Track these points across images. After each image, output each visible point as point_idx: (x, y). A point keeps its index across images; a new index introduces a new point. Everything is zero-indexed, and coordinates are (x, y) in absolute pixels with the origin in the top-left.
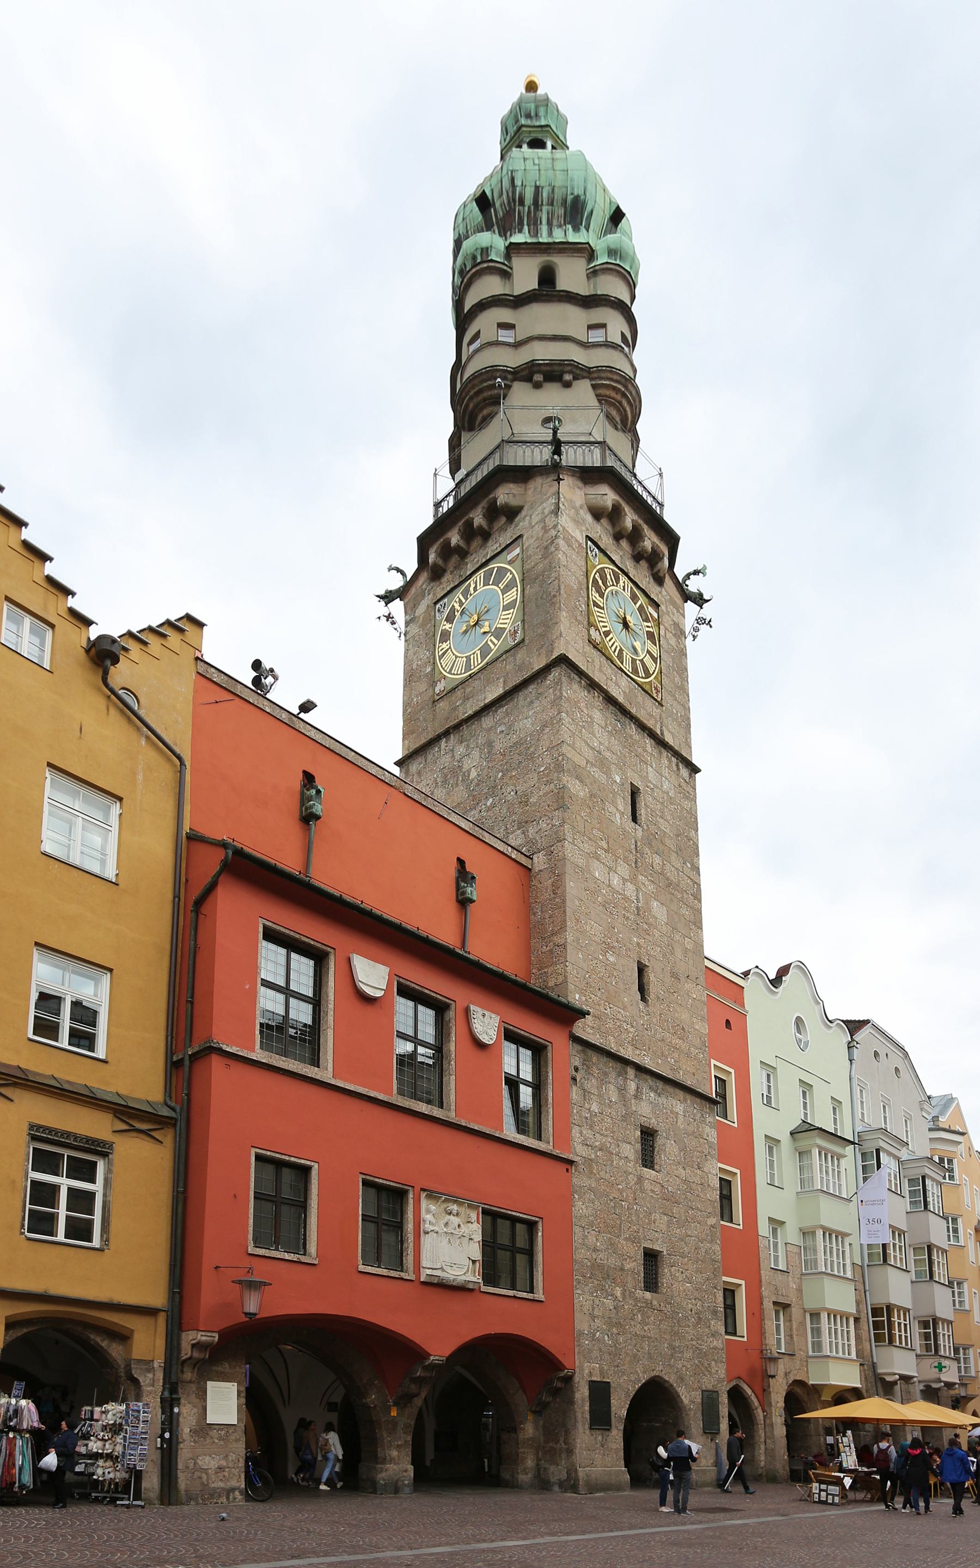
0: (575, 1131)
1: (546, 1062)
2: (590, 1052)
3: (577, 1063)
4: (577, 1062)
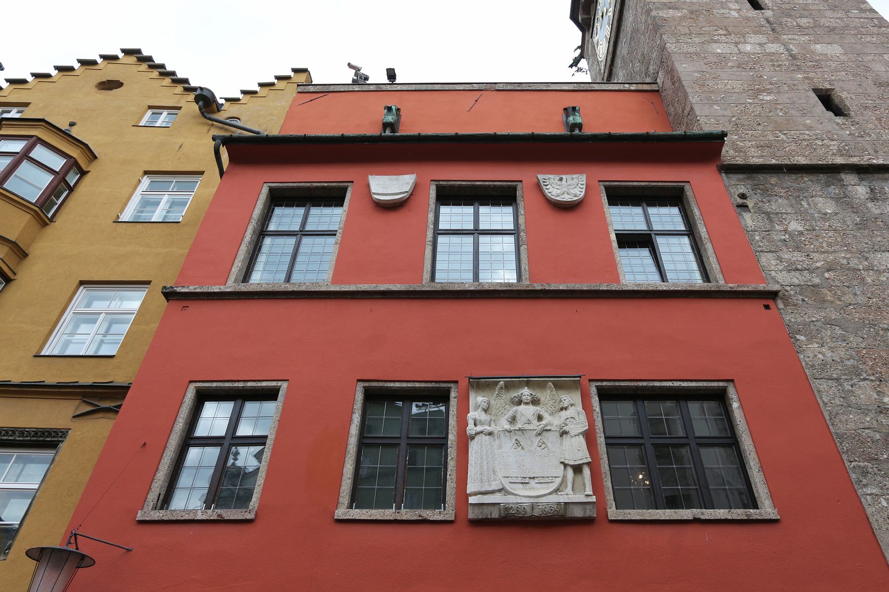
0: (767, 260)
1: (688, 203)
2: (761, 177)
3: (741, 191)
4: (742, 190)
